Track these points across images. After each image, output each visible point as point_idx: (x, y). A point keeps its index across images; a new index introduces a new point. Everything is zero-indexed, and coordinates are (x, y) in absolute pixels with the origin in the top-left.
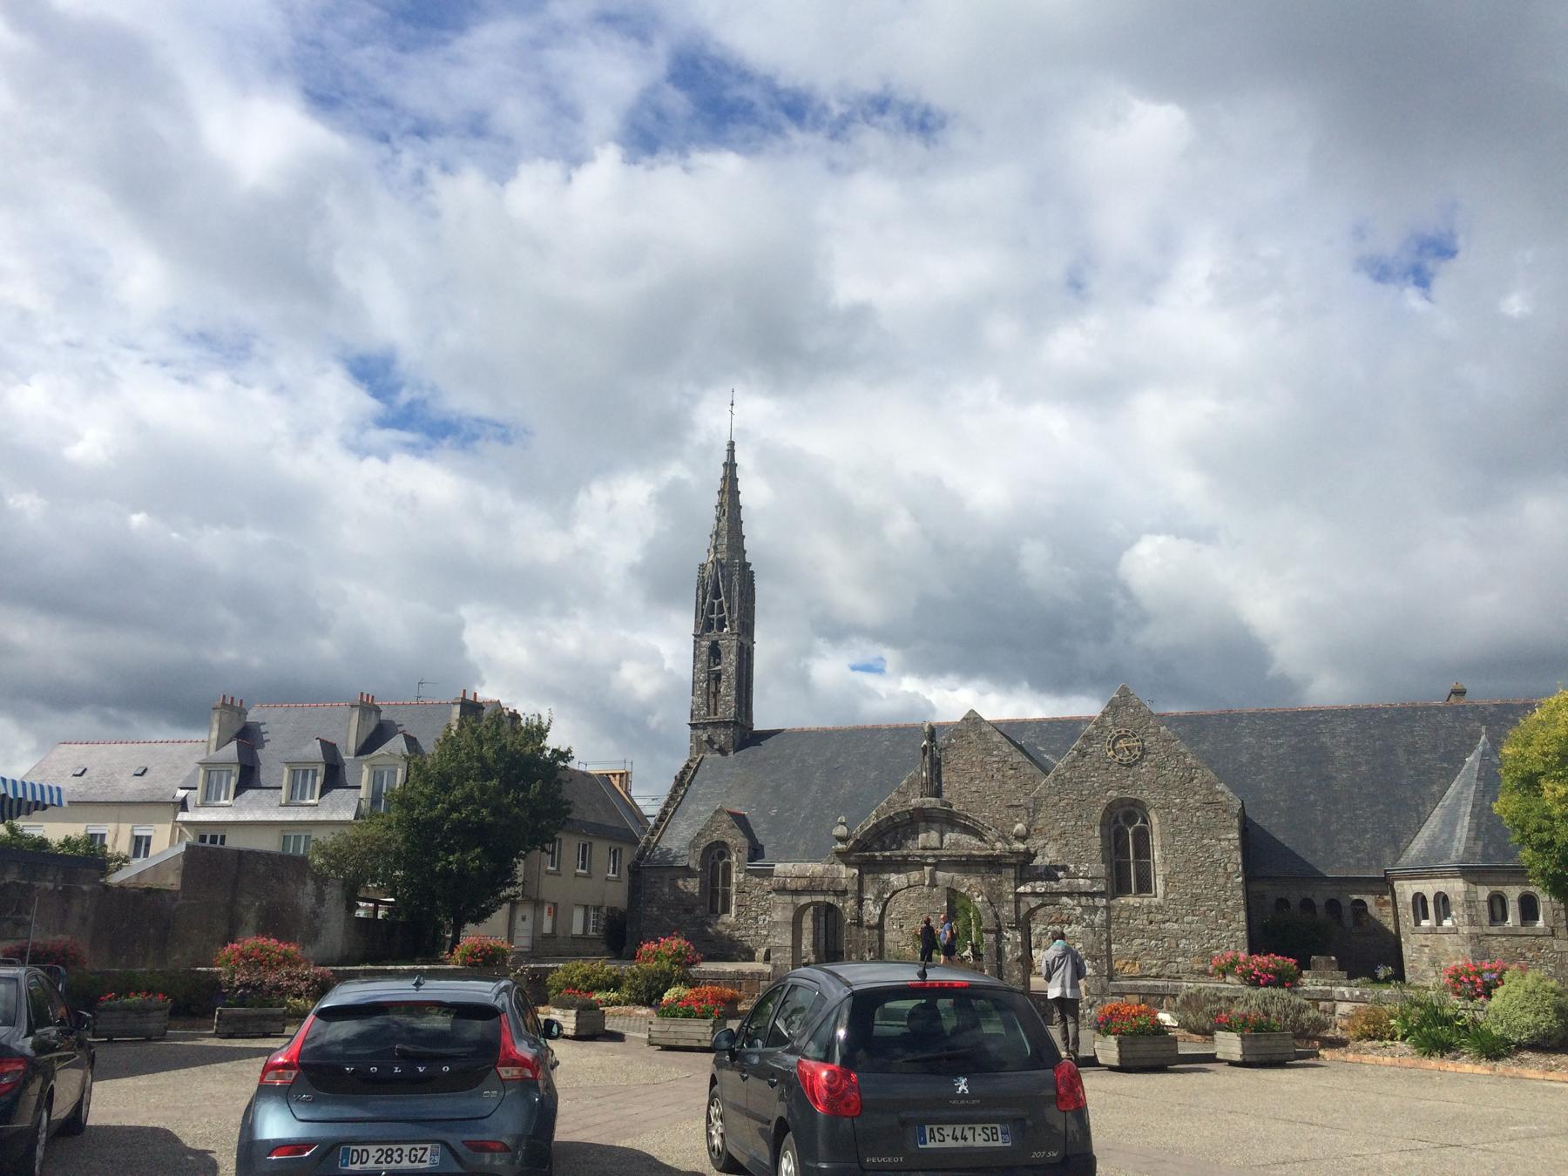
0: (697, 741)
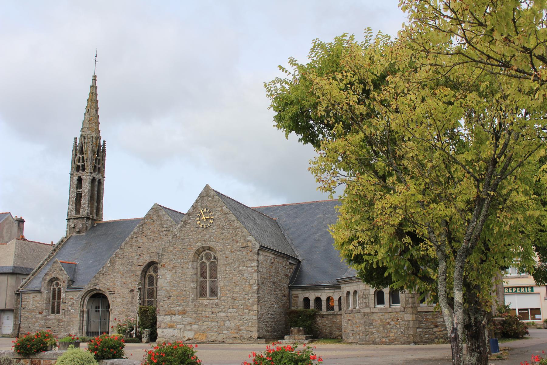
0: (69, 226)
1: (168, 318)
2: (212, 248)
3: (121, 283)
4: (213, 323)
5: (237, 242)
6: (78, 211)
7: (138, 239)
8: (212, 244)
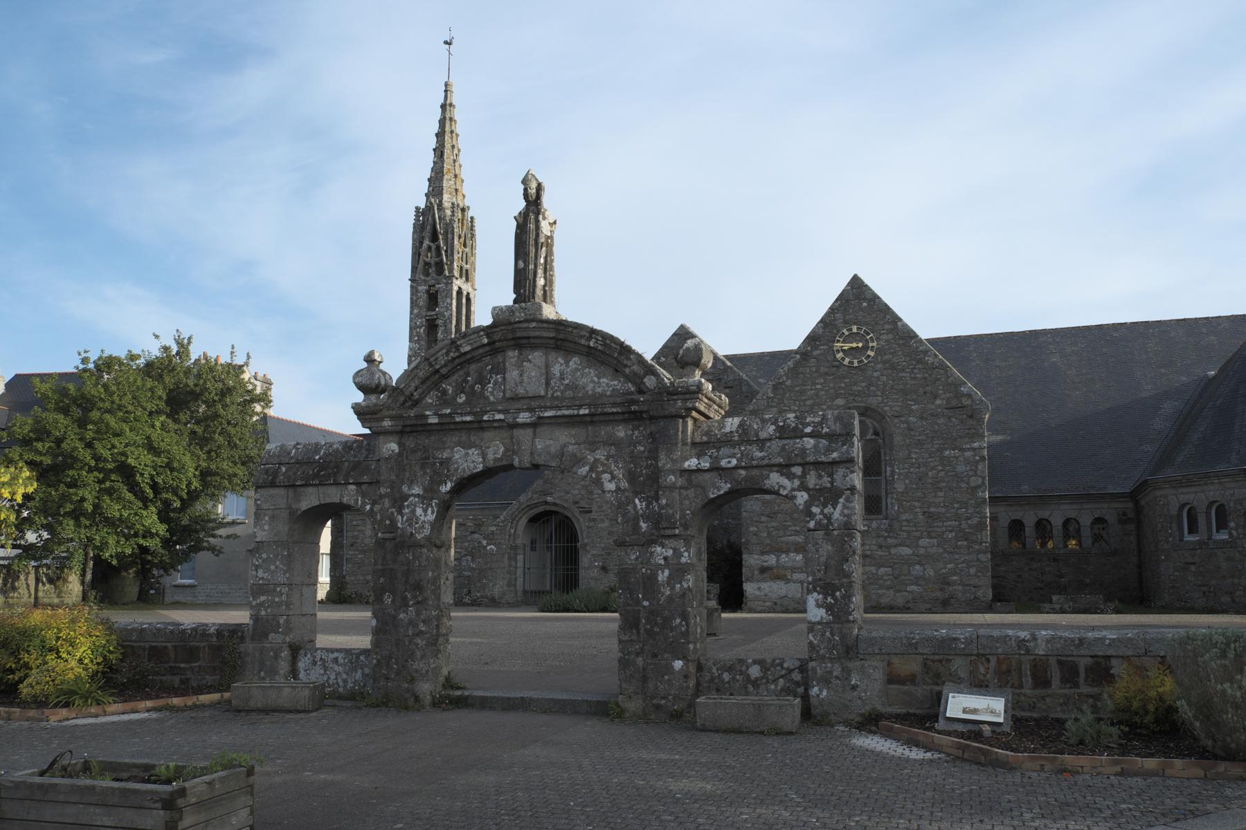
2: (874, 411)
4: (882, 570)
5: (935, 397)
8: (874, 402)
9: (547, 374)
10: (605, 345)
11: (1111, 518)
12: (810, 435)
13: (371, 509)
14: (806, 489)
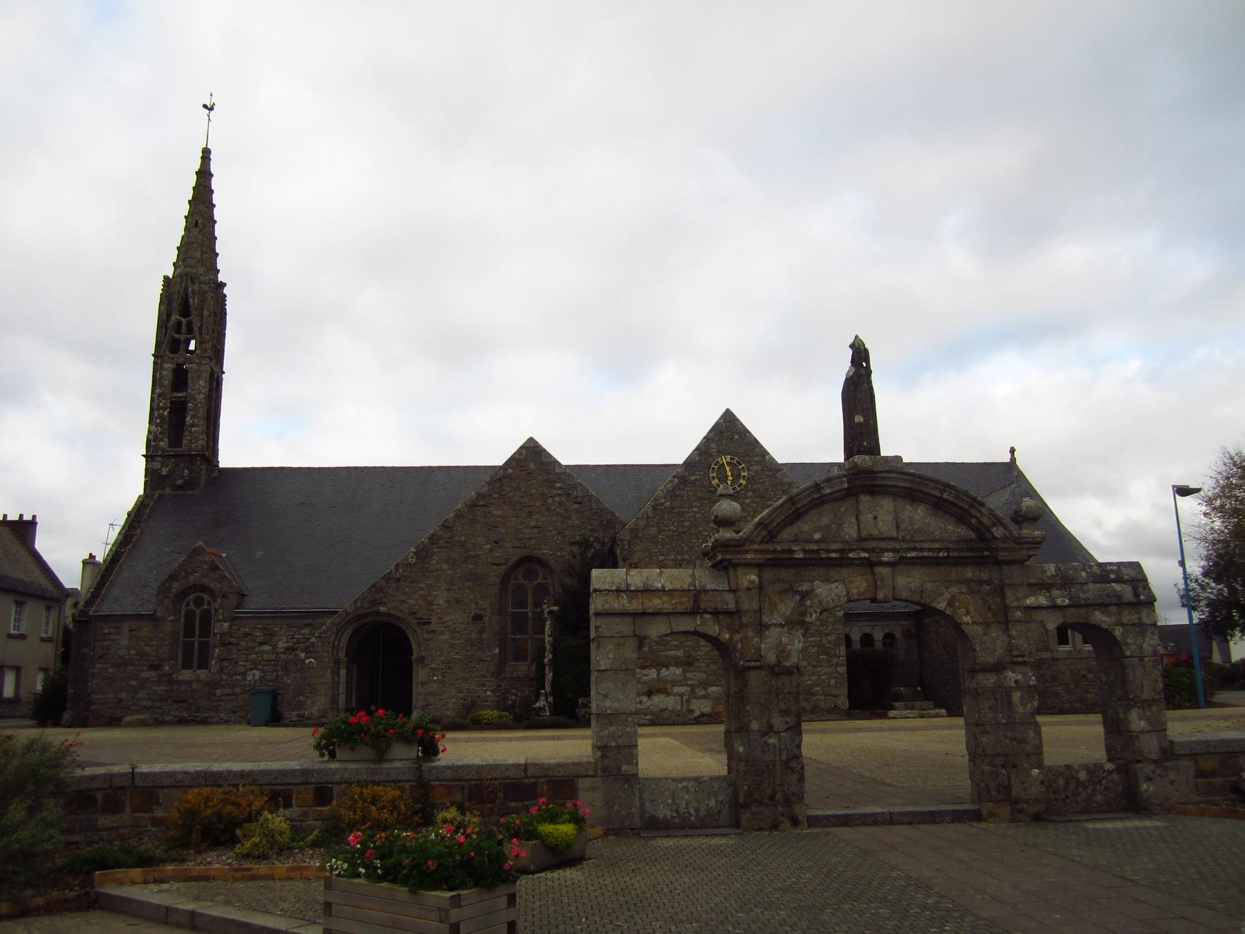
1: (653, 673)
3: (448, 602)
6: (176, 440)
7: (491, 508)
9: (896, 518)
10: (957, 497)
11: (898, 634)
12: (1115, 581)
13: (731, 638)
14: (1123, 625)
